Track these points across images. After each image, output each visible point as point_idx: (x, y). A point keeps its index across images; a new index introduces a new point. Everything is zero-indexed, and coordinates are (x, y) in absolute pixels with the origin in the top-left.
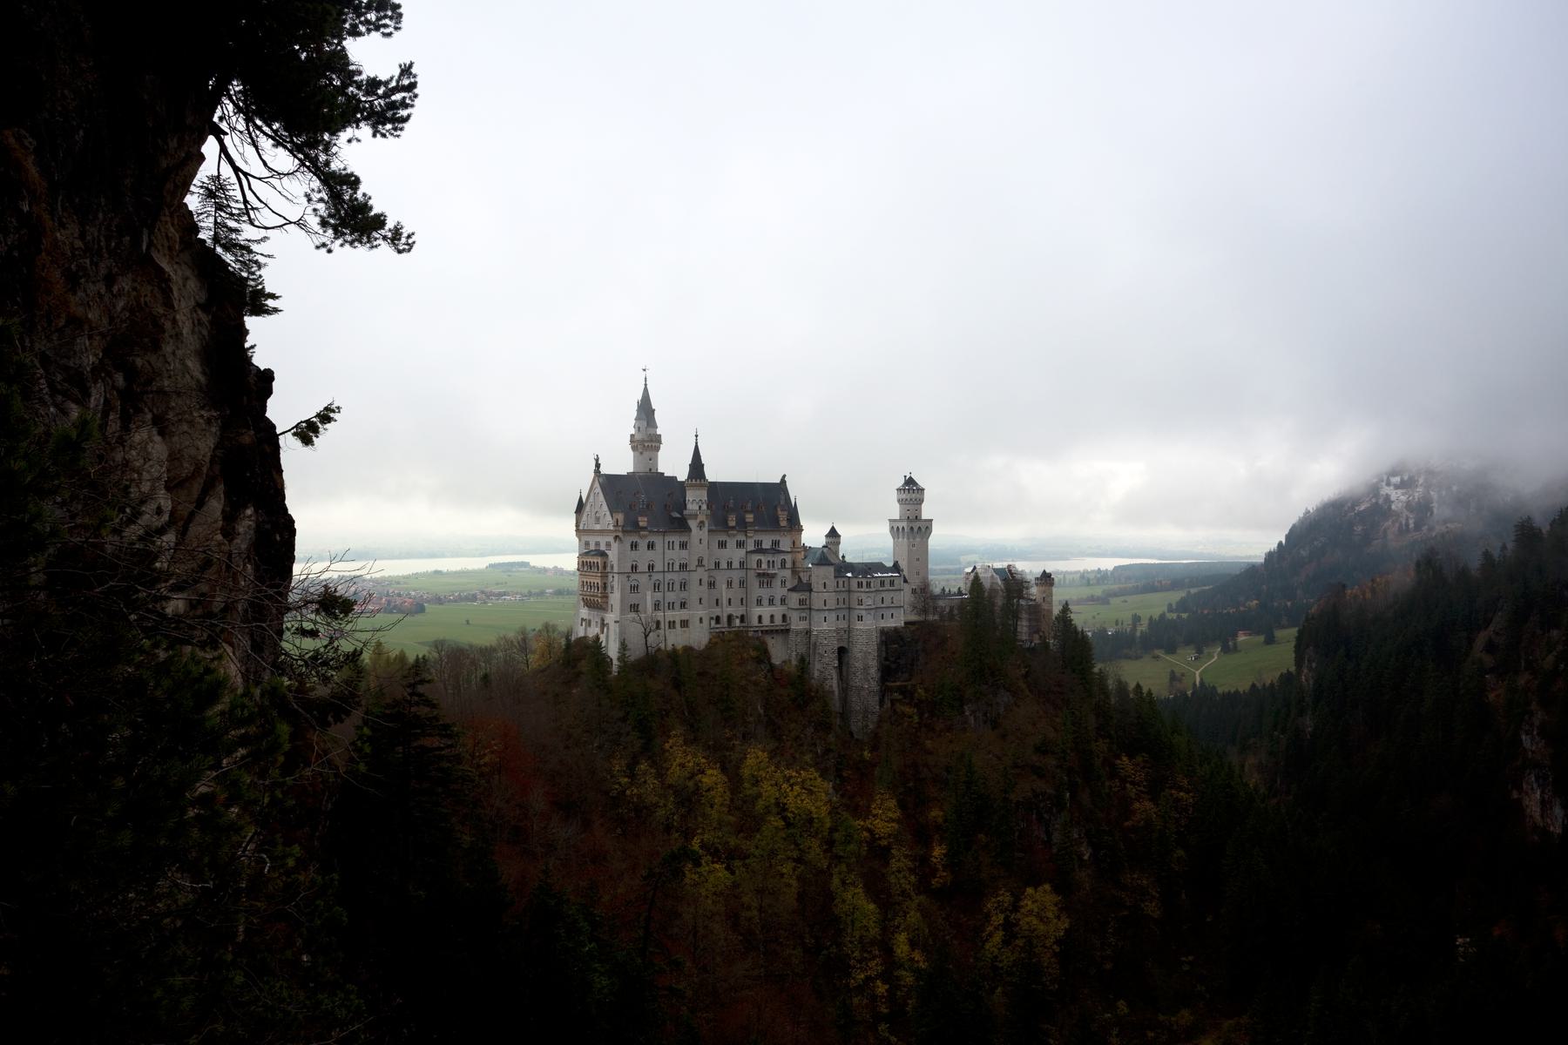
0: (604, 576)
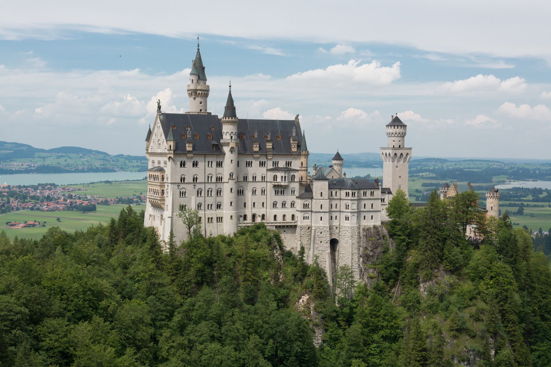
0: (162, 185)
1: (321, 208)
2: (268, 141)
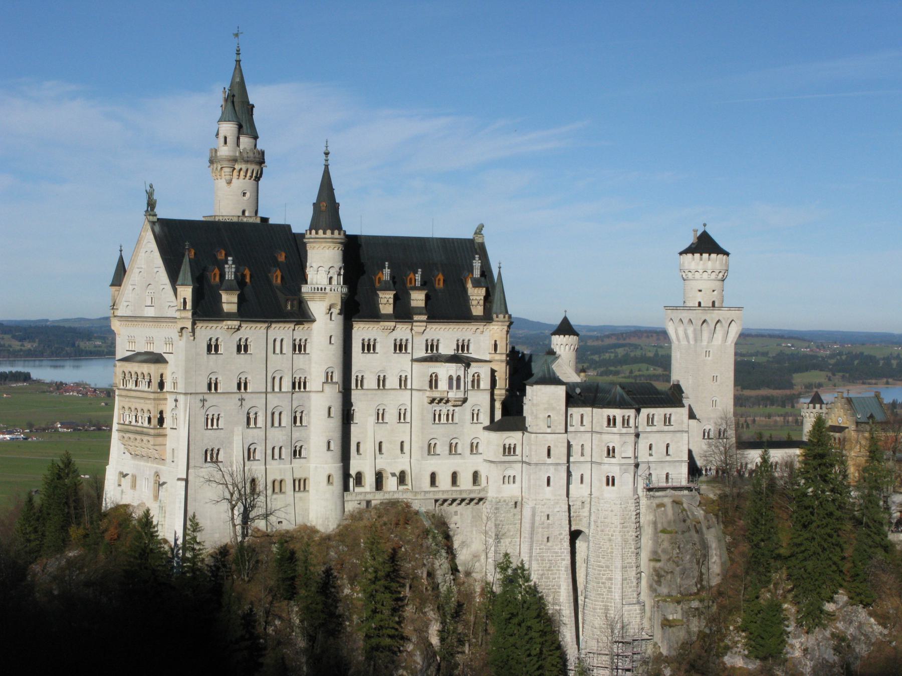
1: (549, 455)
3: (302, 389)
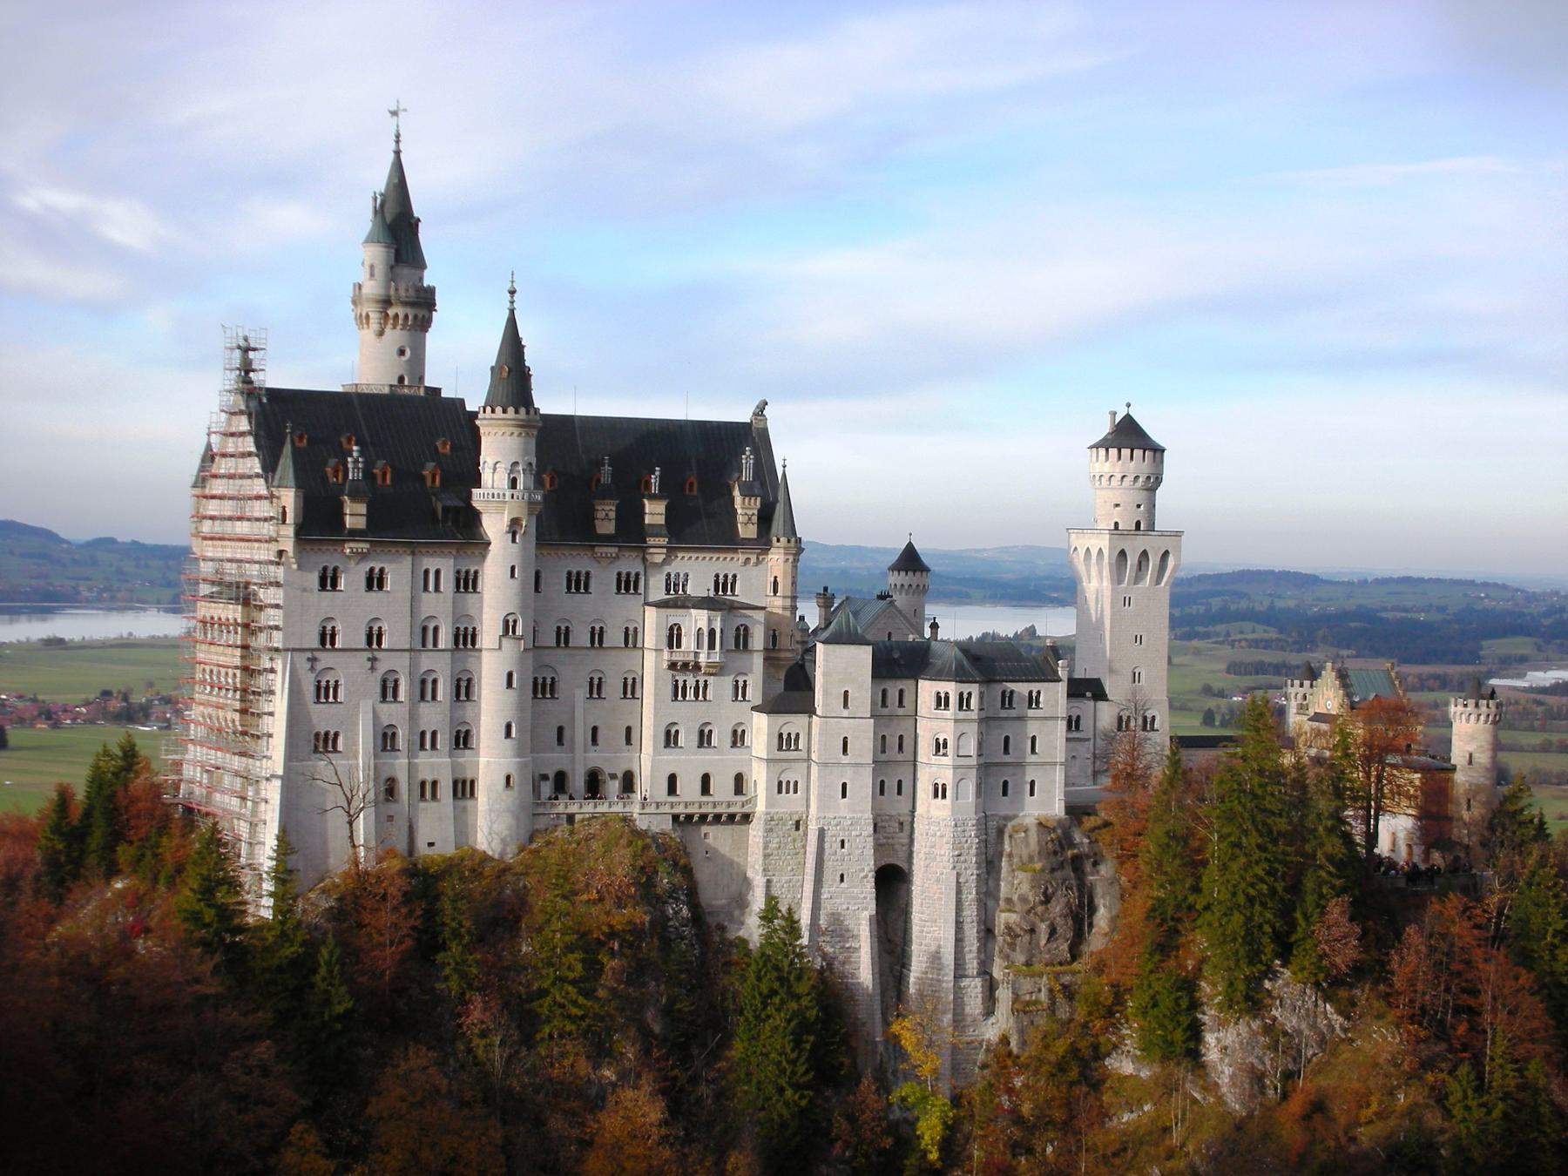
2: (652, 497)
3: (469, 646)
